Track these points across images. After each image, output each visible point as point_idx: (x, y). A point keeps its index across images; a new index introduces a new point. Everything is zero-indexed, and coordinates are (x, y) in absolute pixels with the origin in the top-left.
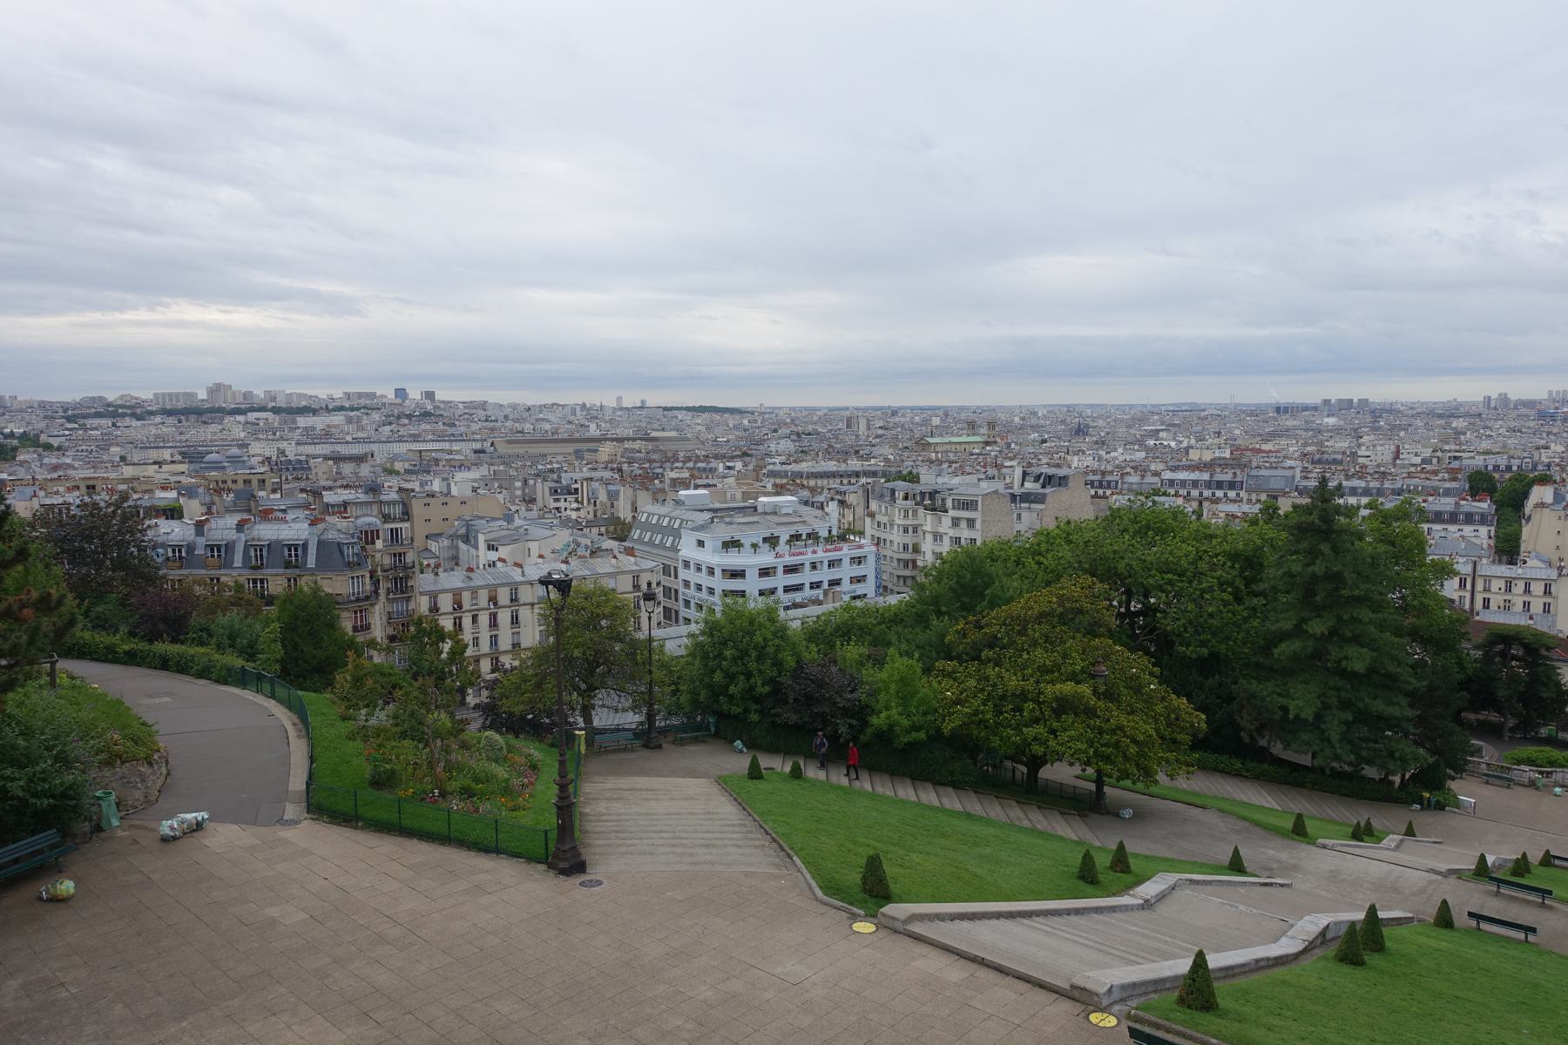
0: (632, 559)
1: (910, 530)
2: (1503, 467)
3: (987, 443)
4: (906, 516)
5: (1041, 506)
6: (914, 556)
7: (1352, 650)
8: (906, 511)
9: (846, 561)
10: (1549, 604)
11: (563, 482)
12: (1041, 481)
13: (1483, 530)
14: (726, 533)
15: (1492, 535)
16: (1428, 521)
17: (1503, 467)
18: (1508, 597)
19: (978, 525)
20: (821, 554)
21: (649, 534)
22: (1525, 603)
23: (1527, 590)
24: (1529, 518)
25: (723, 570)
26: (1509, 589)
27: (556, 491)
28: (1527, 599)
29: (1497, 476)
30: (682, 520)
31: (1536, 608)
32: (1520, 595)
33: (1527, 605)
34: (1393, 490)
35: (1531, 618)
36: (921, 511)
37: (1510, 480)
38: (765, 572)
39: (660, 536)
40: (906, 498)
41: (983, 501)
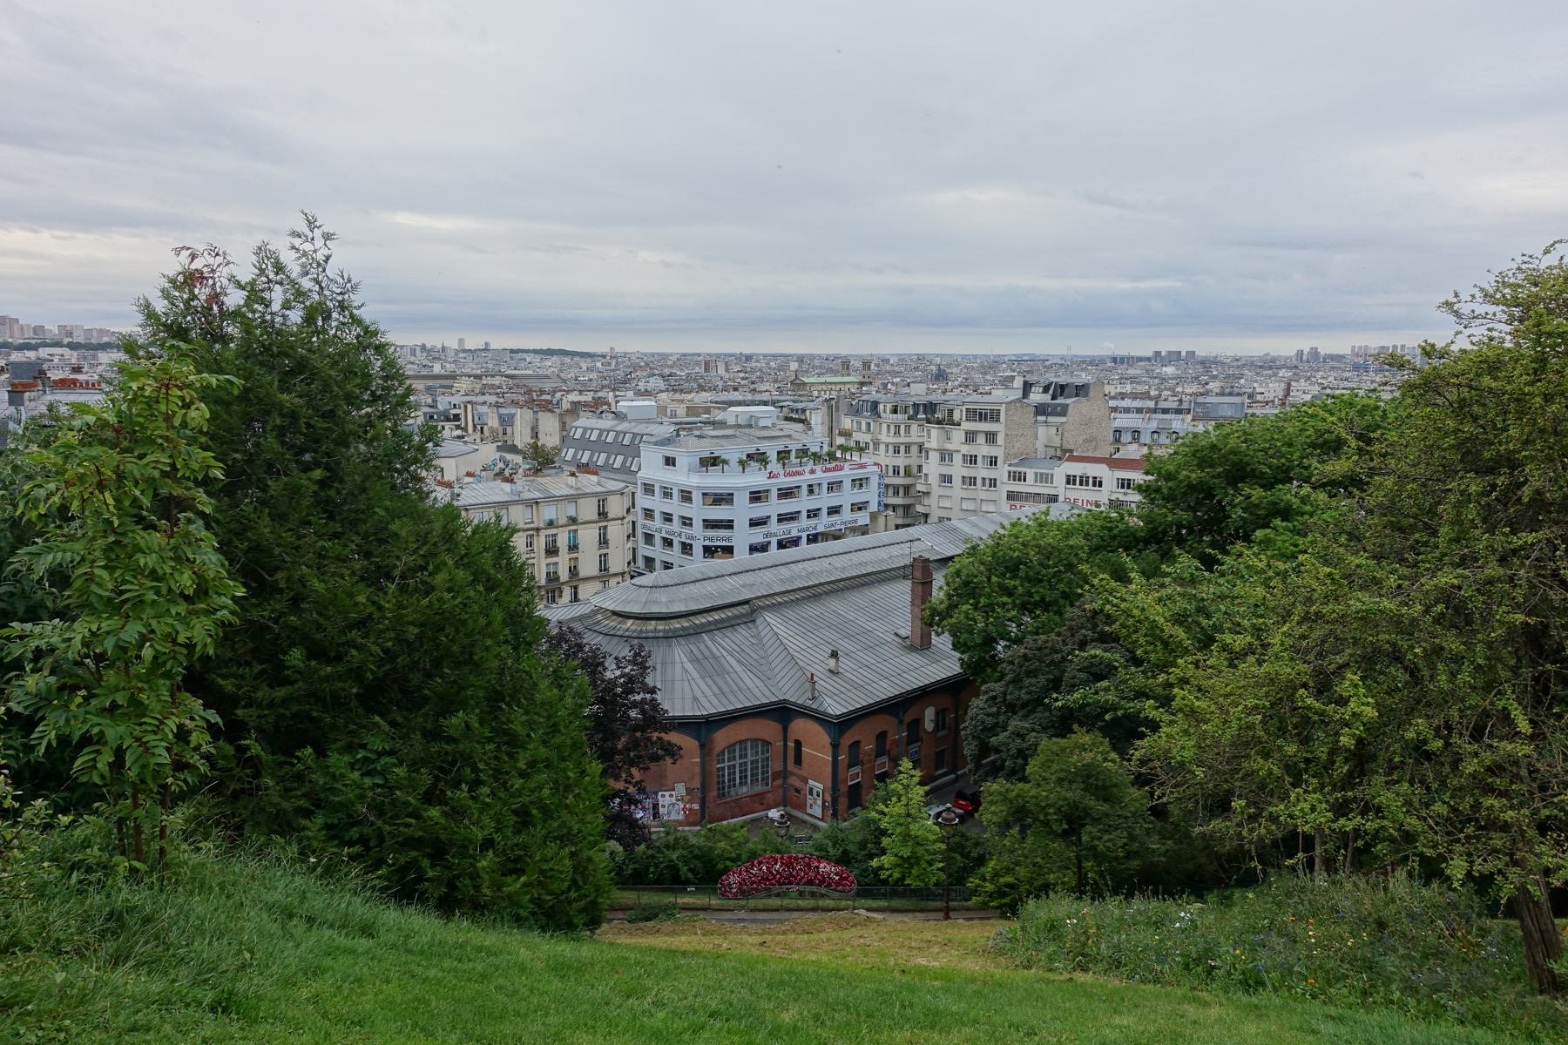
0: (594, 478)
1: (902, 449)
3: (862, 384)
4: (897, 432)
5: (1063, 419)
6: (908, 481)
8: (897, 427)
9: (847, 484)
11: (440, 406)
12: (1051, 392)
14: (706, 448)
19: (1000, 439)
20: (821, 475)
21: (587, 454)
25: (704, 494)
27: (431, 417)
30: (635, 435)
36: (914, 427)
38: (757, 497)
39: (603, 456)
40: (895, 411)
41: (1007, 410)
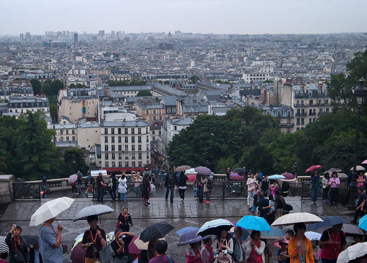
2: (42, 77)
7: (45, 164)
10: (74, 137)
13: (46, 109)
15: (49, 109)
16: (26, 107)
17: (42, 77)
18: (61, 136)
22: (67, 137)
23: (67, 133)
24: (60, 103)
26: (62, 133)
28: (67, 136)
29: (40, 80)
31: (71, 139)
32: (64, 135)
33: (68, 138)
34: (7, 92)
35: (70, 143)
37: (45, 82)
